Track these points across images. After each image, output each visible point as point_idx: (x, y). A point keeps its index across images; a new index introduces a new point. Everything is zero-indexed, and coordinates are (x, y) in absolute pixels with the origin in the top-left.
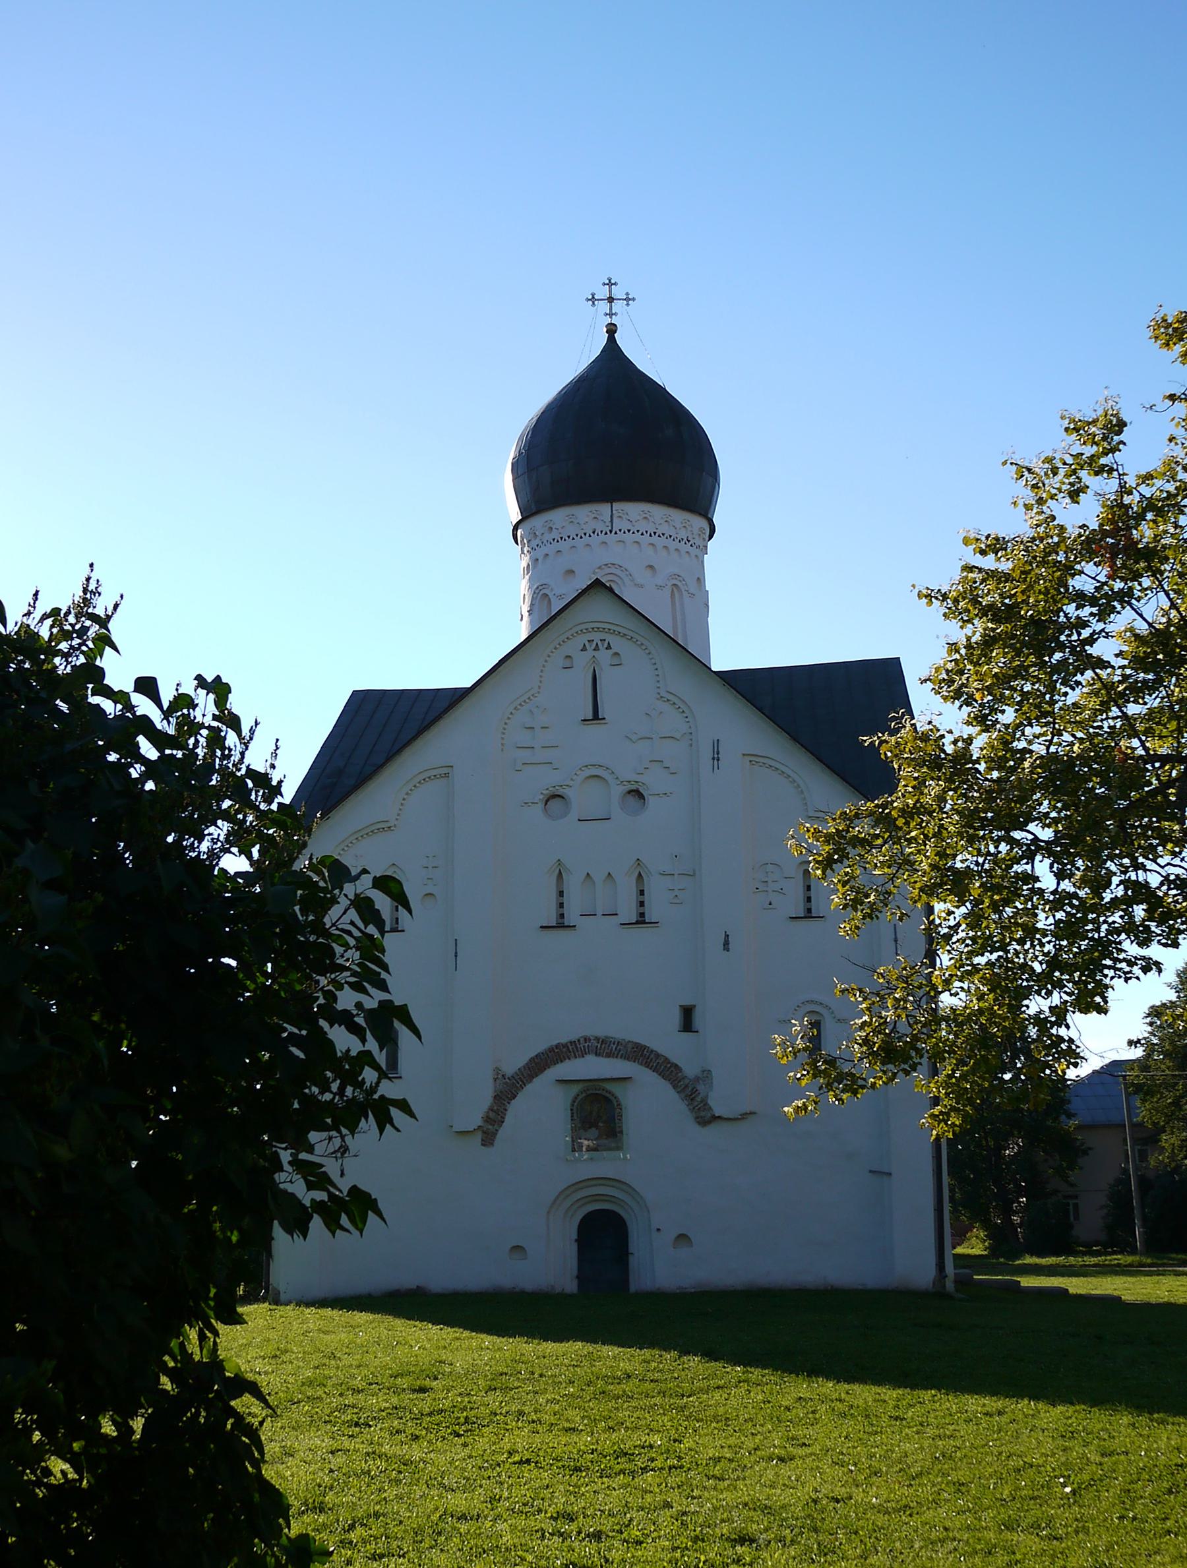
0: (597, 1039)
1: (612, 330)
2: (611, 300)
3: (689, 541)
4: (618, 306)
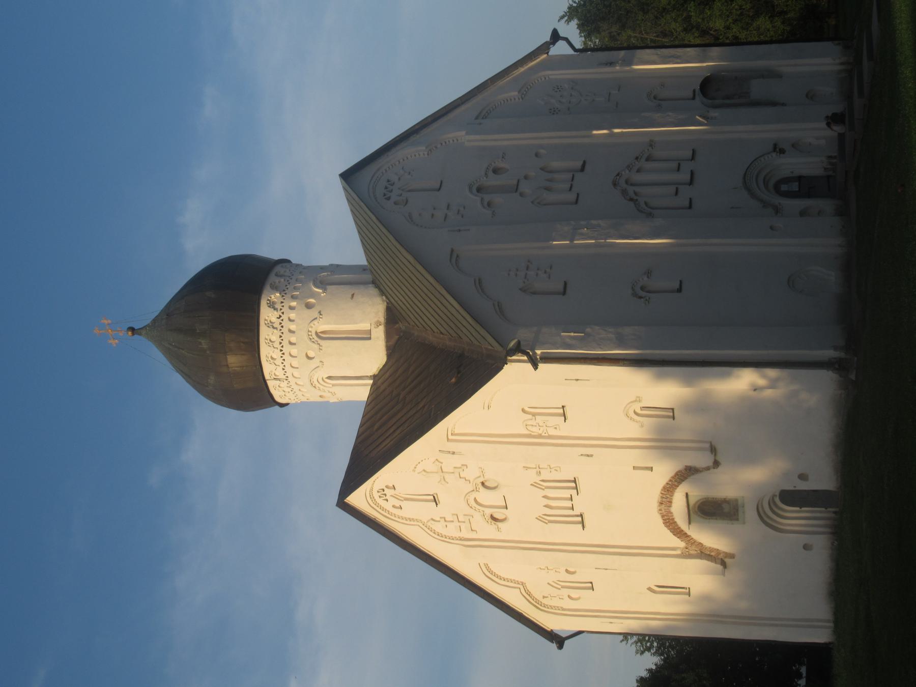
0: (659, 506)
3: (280, 316)
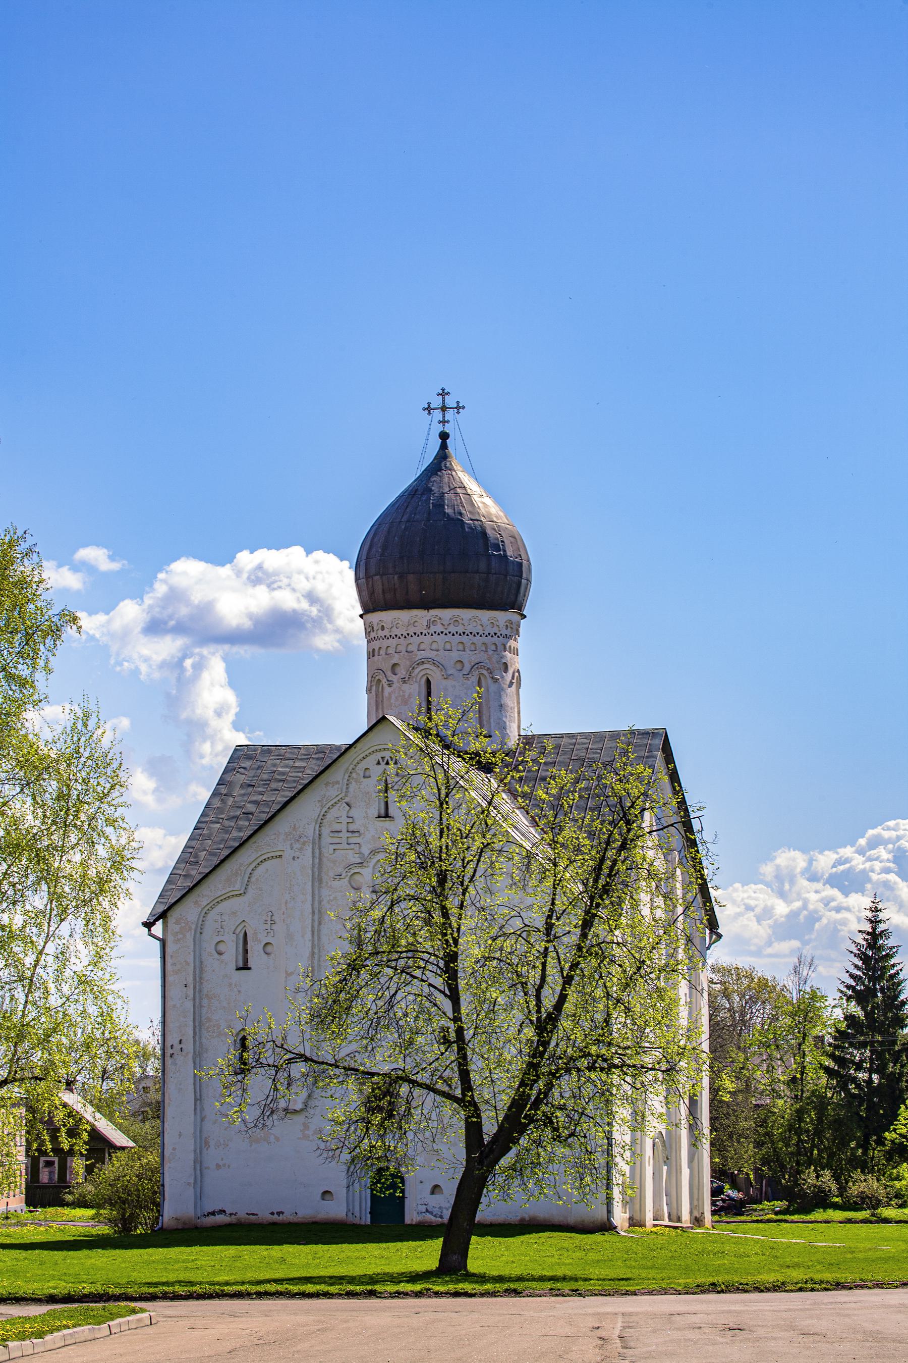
1: (444, 436)
2: (444, 408)
4: (450, 414)
